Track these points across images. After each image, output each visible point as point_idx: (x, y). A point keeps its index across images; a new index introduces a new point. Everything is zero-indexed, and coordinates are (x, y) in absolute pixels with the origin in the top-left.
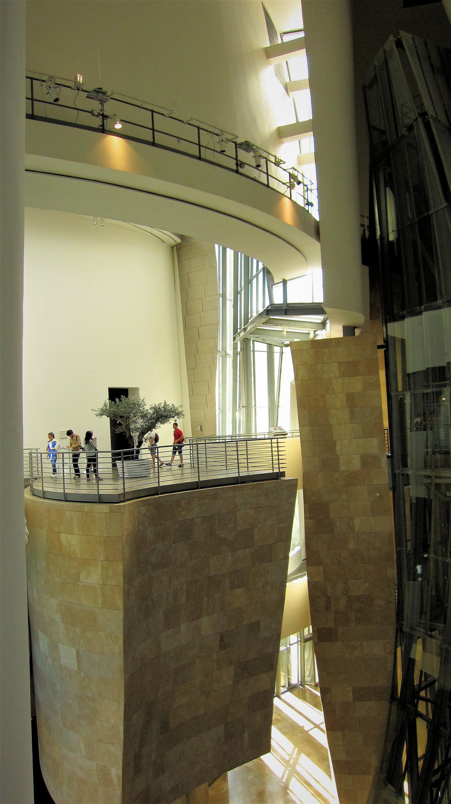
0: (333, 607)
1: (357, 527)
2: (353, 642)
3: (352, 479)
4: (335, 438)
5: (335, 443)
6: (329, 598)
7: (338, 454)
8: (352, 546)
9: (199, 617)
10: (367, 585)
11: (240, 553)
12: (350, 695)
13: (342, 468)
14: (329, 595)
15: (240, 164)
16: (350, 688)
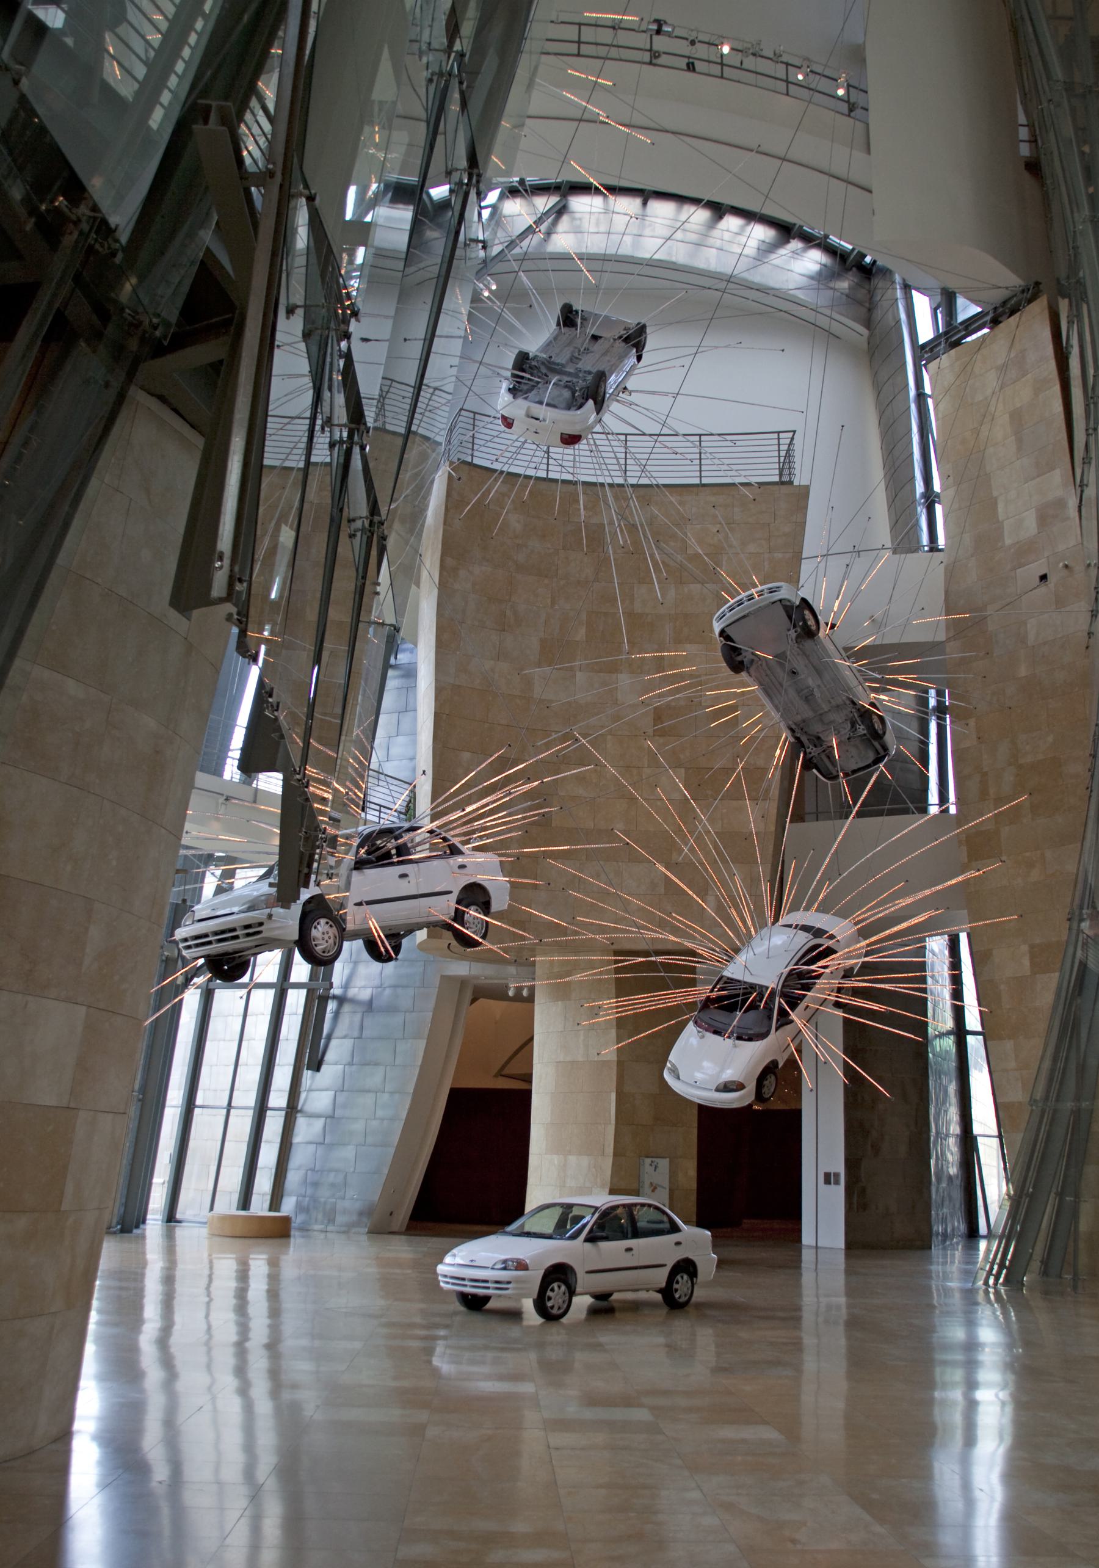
0: (992, 791)
1: (1031, 637)
2: (1028, 854)
3: (1025, 551)
4: (995, 494)
5: (996, 499)
6: (986, 774)
7: (1000, 519)
8: (1023, 671)
9: (613, 668)
10: (1050, 739)
11: (695, 588)
12: (1026, 962)
13: (1008, 541)
14: (985, 769)
15: (655, 55)
16: (1025, 948)
